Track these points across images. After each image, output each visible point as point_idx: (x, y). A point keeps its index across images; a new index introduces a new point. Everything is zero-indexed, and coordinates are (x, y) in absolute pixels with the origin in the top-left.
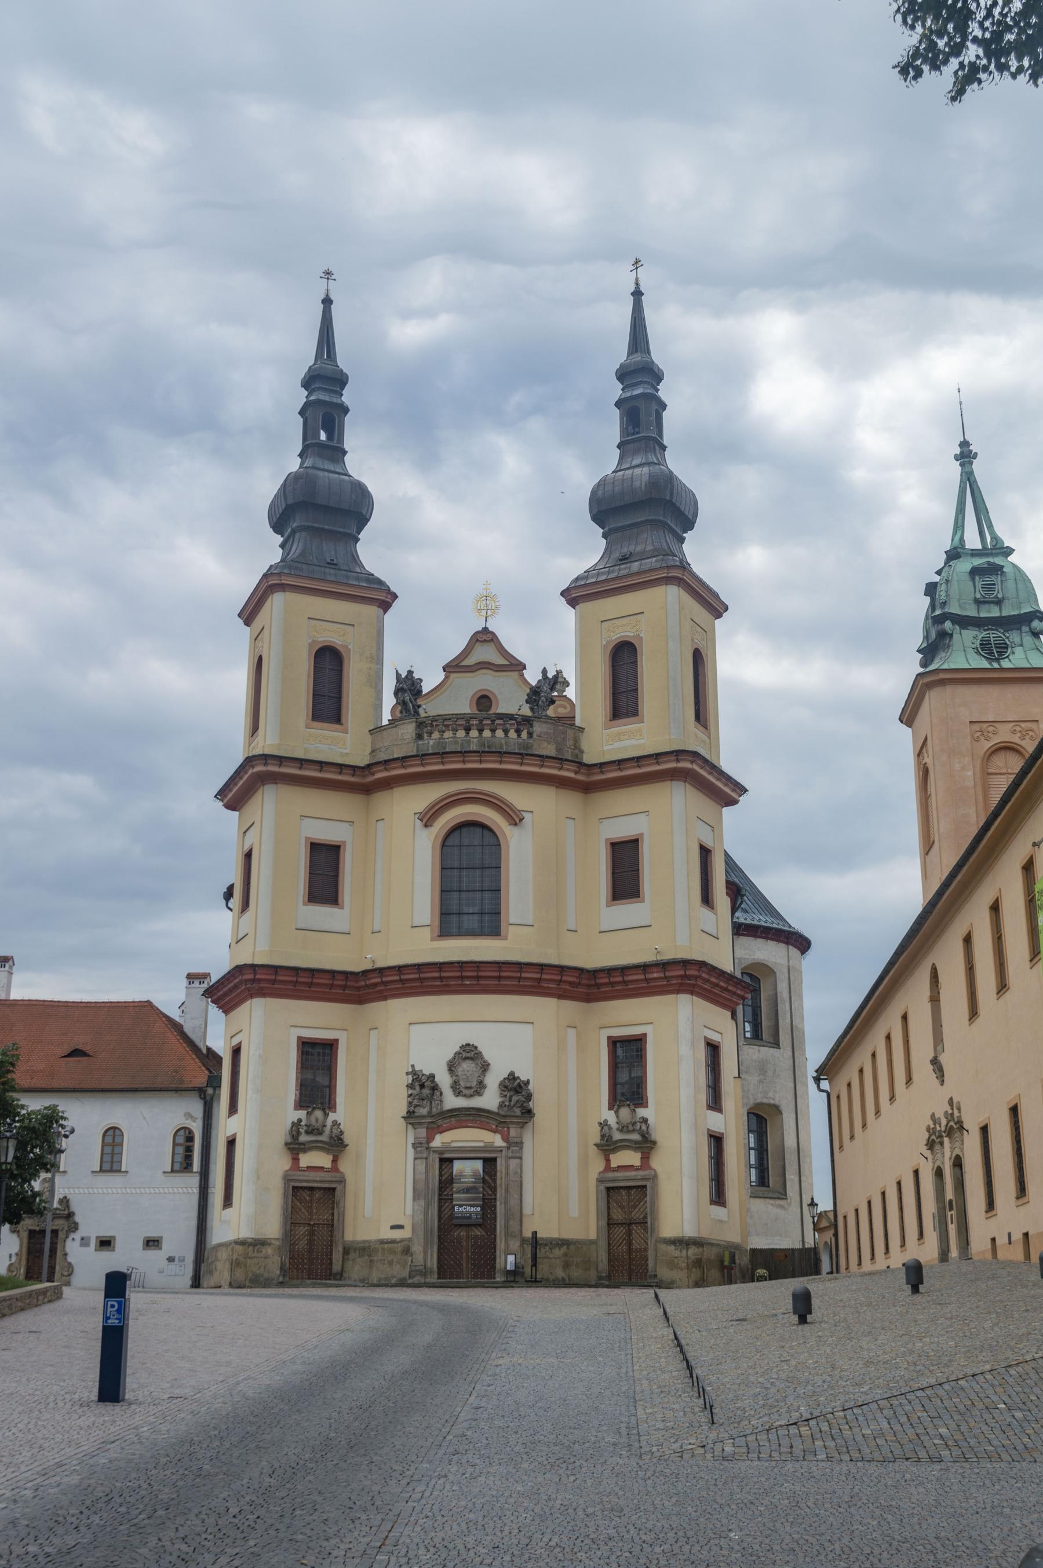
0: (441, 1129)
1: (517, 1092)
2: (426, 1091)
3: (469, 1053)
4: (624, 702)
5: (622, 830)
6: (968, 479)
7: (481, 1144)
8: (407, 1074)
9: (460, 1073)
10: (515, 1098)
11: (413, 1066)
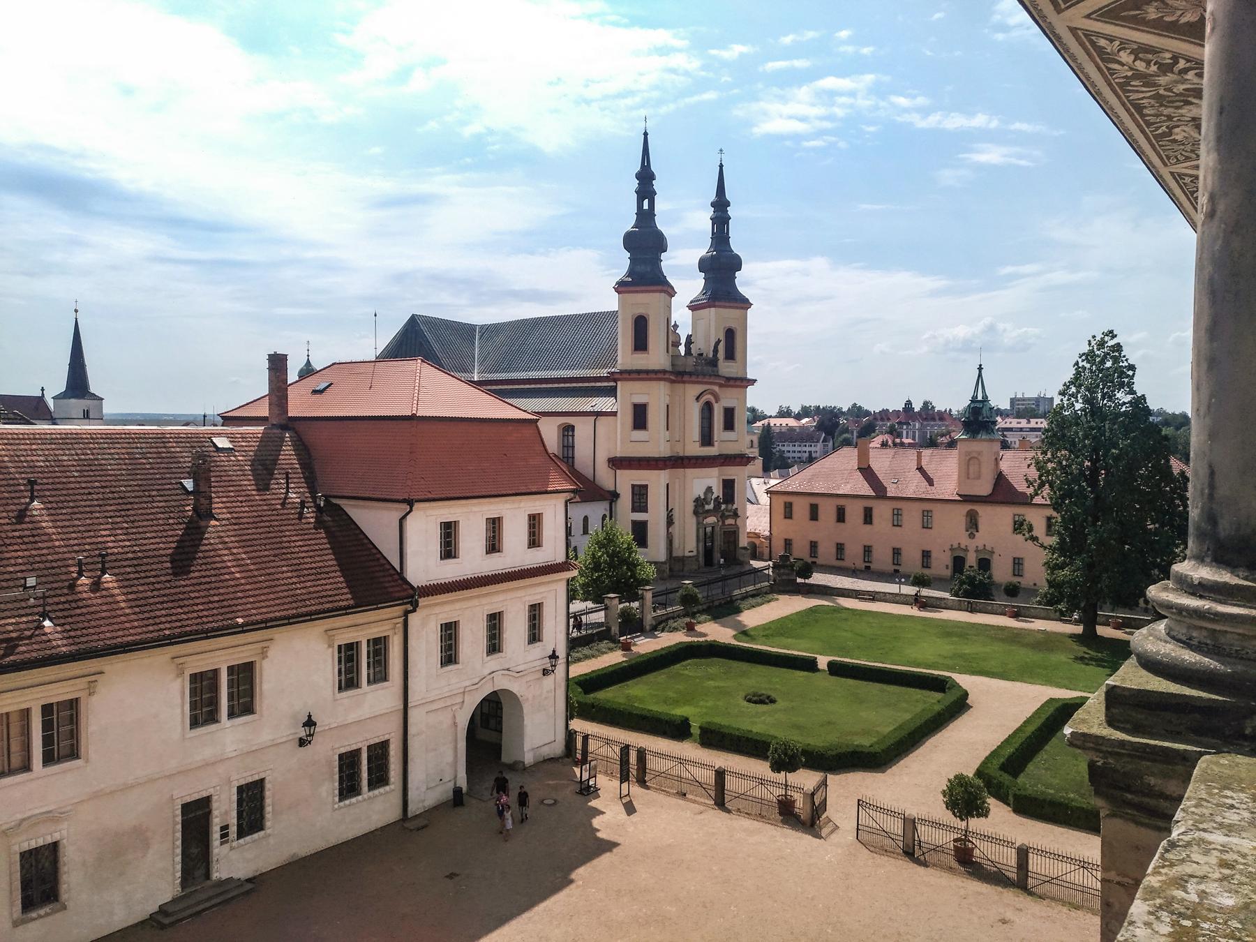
3: (709, 489)
4: (730, 355)
5: (729, 404)
6: (980, 375)
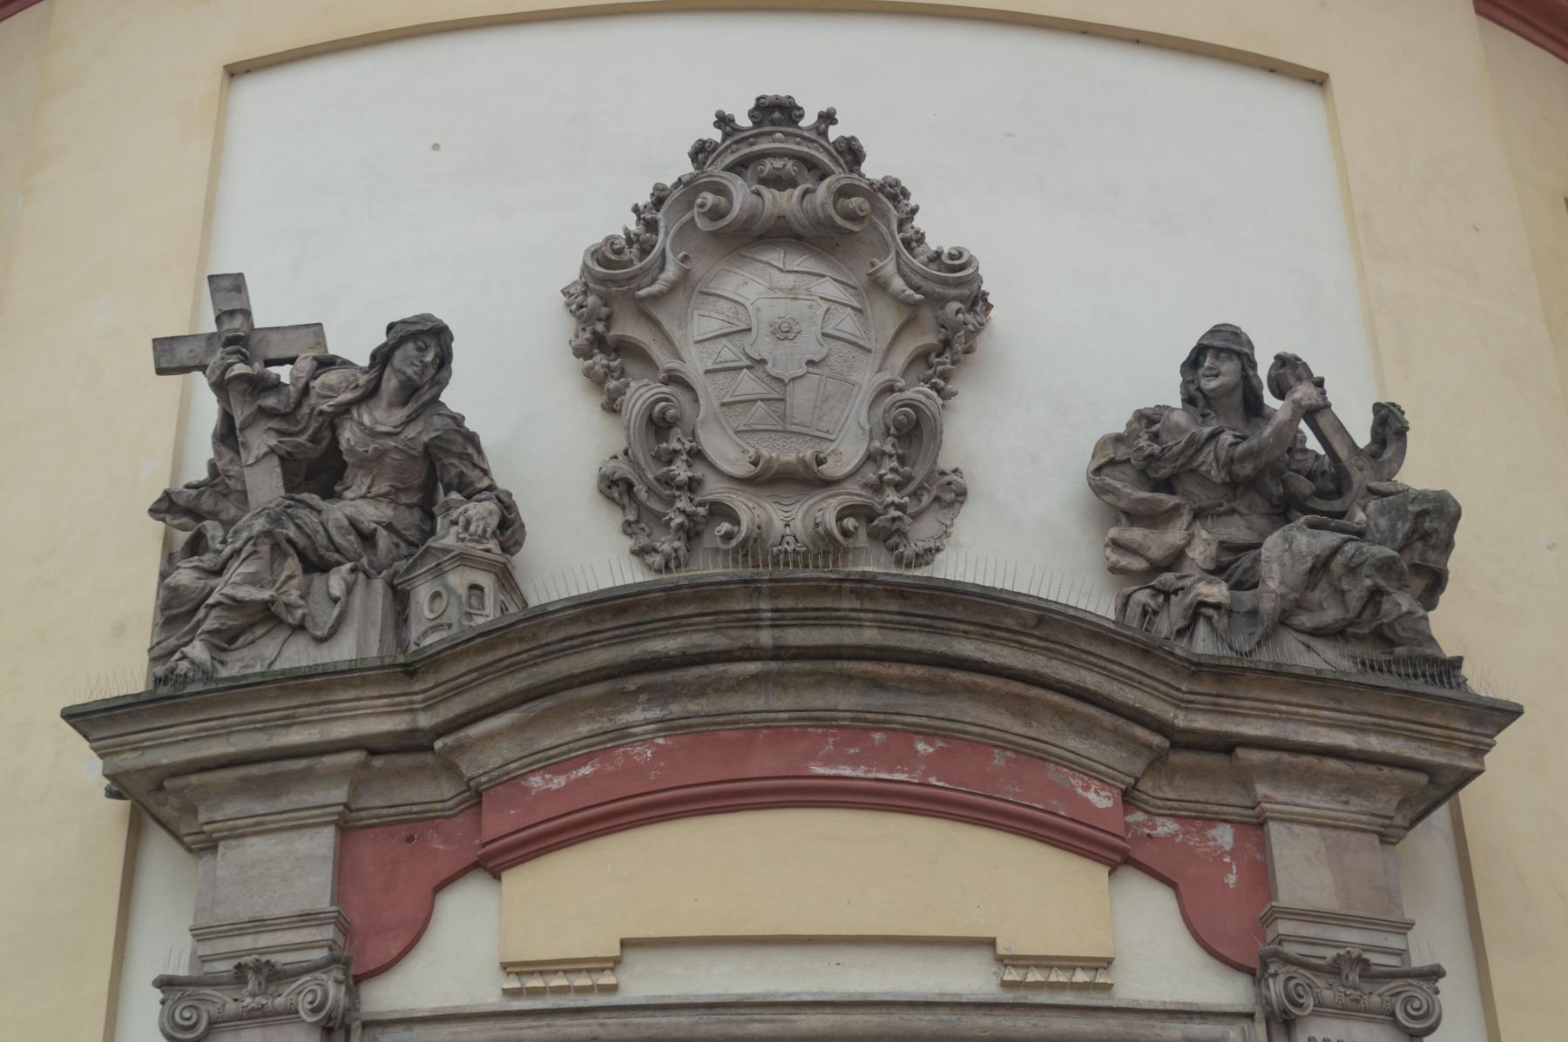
0: (499, 822)
1: (1284, 510)
2: (360, 505)
7: (970, 979)
8: (170, 358)
9: (694, 364)
10: (1286, 552)
11: (228, 288)
